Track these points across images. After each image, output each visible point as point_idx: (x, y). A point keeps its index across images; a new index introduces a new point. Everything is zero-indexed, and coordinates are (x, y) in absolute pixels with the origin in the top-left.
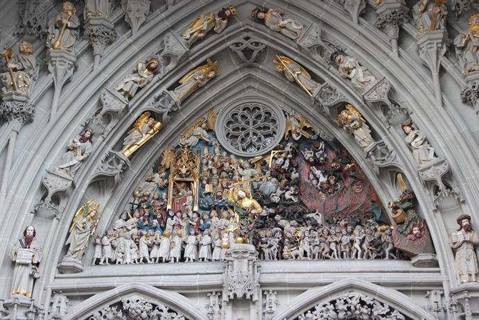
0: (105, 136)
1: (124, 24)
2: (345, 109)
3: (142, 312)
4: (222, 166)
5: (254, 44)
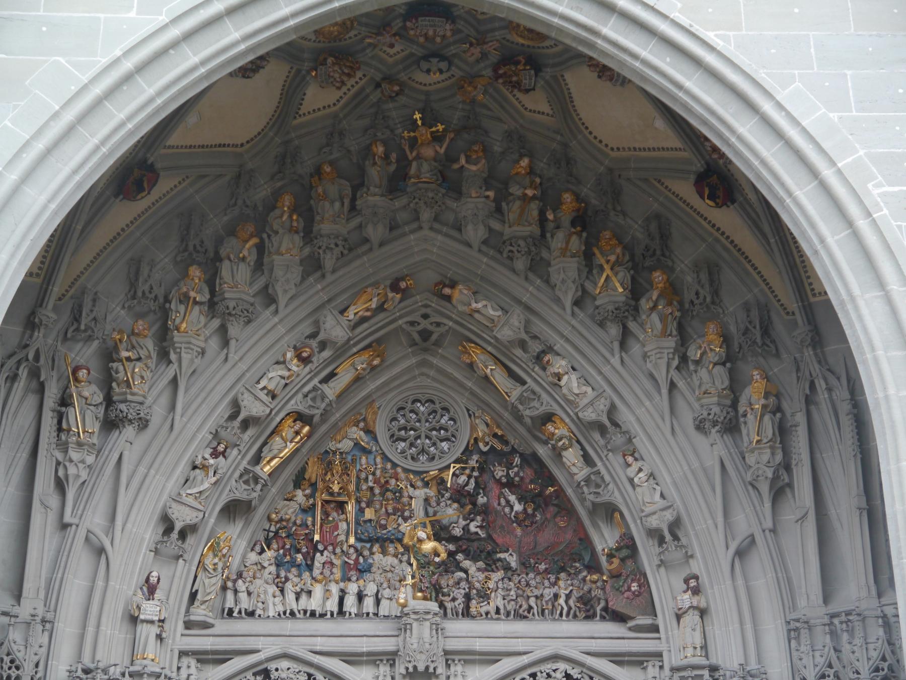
1: (269, 298)
4: (387, 482)
5: (434, 325)
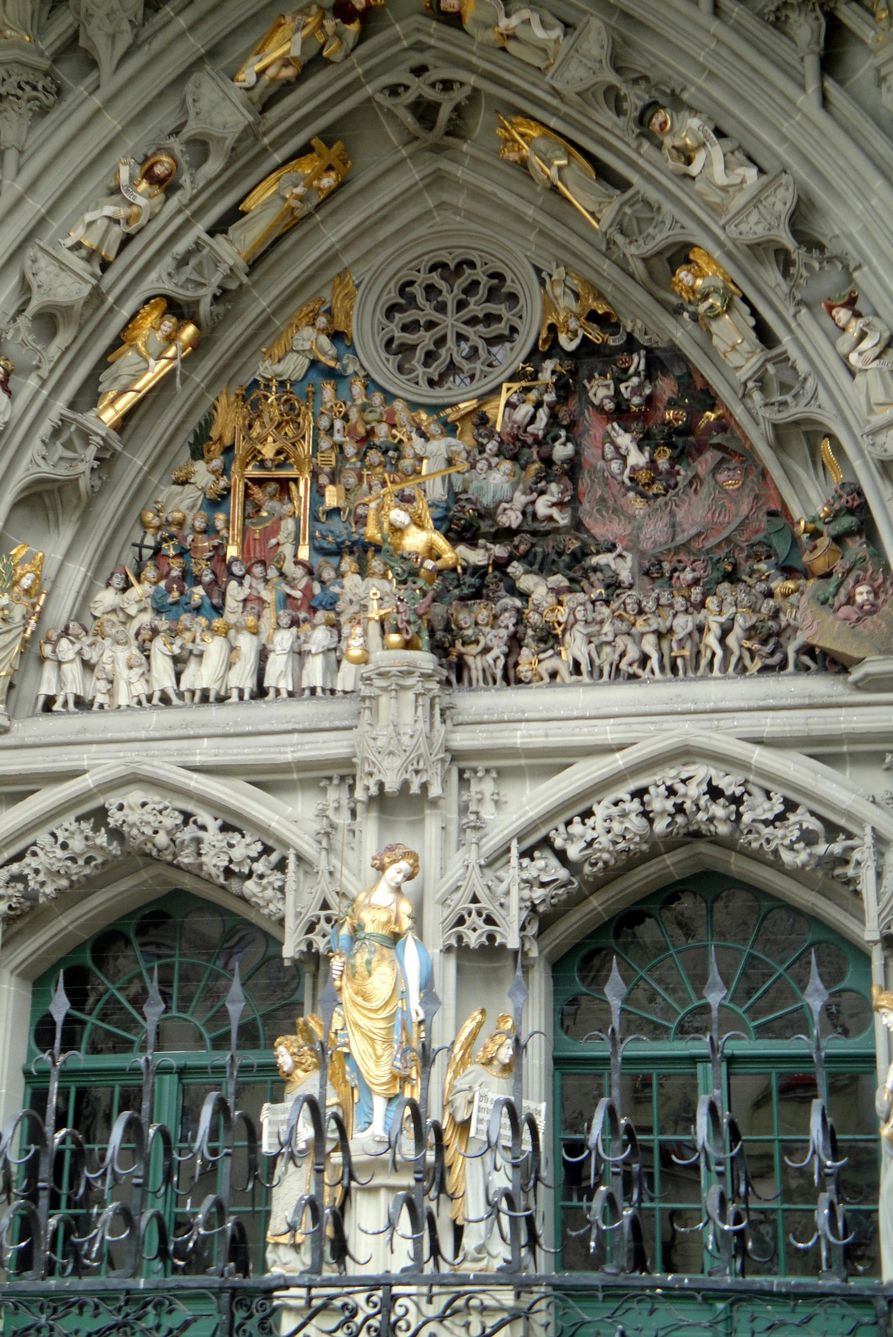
0: (44, 373)
2: (688, 261)
3: (156, 832)
4: (371, 433)
5: (439, 86)
